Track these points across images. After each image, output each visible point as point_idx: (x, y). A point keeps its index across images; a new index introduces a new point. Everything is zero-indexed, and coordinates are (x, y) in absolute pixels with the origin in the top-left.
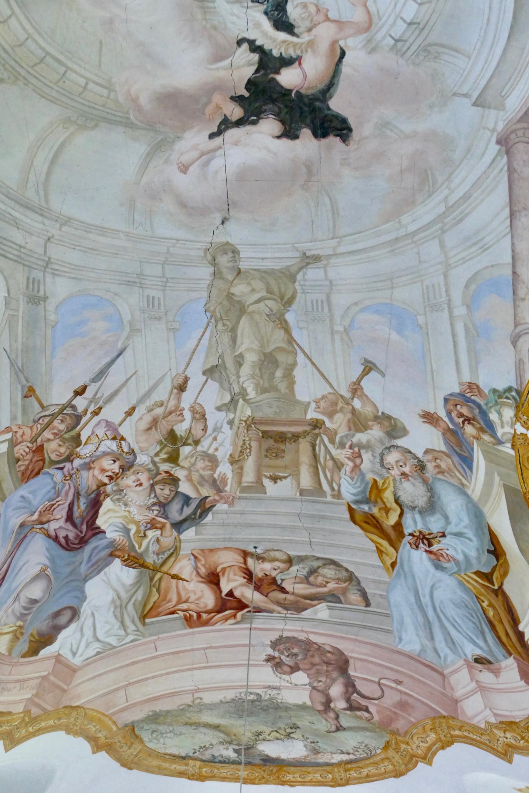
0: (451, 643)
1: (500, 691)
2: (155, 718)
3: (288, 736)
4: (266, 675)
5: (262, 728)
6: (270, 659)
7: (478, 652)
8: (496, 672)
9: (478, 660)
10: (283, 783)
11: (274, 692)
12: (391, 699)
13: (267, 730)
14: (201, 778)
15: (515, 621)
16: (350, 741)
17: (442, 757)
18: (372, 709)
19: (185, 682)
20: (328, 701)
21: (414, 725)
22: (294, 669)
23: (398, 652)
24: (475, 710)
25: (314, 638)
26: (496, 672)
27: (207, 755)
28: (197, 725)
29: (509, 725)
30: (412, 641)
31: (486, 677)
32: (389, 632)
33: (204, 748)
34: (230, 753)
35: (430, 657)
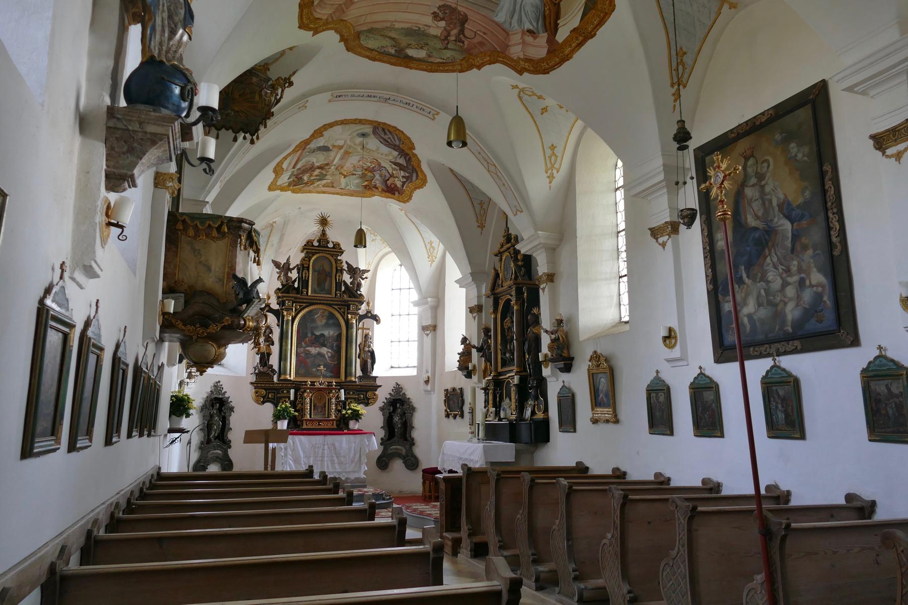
0: (520, 21)
1: (534, 46)
2: (371, 31)
3: (422, 48)
4: (429, 20)
5: (414, 43)
6: (434, 13)
7: (531, 28)
8: (535, 38)
9: (529, 31)
10: (407, 67)
11: (426, 28)
12: (477, 39)
13: (414, 43)
14: (374, 60)
15: (558, 16)
16: (448, 54)
17: (487, 68)
18: (466, 43)
19: (391, 17)
20: (449, 35)
21: (481, 52)
22: (442, 19)
23: (494, 22)
24: (516, 51)
25: (459, 8)
26: (535, 38)
27: (383, 50)
28: (386, 36)
29: (528, 60)
30: (501, 17)
31: (529, 39)
32: (494, 11)
33: (383, 47)
34: (393, 51)
35: (506, 26)
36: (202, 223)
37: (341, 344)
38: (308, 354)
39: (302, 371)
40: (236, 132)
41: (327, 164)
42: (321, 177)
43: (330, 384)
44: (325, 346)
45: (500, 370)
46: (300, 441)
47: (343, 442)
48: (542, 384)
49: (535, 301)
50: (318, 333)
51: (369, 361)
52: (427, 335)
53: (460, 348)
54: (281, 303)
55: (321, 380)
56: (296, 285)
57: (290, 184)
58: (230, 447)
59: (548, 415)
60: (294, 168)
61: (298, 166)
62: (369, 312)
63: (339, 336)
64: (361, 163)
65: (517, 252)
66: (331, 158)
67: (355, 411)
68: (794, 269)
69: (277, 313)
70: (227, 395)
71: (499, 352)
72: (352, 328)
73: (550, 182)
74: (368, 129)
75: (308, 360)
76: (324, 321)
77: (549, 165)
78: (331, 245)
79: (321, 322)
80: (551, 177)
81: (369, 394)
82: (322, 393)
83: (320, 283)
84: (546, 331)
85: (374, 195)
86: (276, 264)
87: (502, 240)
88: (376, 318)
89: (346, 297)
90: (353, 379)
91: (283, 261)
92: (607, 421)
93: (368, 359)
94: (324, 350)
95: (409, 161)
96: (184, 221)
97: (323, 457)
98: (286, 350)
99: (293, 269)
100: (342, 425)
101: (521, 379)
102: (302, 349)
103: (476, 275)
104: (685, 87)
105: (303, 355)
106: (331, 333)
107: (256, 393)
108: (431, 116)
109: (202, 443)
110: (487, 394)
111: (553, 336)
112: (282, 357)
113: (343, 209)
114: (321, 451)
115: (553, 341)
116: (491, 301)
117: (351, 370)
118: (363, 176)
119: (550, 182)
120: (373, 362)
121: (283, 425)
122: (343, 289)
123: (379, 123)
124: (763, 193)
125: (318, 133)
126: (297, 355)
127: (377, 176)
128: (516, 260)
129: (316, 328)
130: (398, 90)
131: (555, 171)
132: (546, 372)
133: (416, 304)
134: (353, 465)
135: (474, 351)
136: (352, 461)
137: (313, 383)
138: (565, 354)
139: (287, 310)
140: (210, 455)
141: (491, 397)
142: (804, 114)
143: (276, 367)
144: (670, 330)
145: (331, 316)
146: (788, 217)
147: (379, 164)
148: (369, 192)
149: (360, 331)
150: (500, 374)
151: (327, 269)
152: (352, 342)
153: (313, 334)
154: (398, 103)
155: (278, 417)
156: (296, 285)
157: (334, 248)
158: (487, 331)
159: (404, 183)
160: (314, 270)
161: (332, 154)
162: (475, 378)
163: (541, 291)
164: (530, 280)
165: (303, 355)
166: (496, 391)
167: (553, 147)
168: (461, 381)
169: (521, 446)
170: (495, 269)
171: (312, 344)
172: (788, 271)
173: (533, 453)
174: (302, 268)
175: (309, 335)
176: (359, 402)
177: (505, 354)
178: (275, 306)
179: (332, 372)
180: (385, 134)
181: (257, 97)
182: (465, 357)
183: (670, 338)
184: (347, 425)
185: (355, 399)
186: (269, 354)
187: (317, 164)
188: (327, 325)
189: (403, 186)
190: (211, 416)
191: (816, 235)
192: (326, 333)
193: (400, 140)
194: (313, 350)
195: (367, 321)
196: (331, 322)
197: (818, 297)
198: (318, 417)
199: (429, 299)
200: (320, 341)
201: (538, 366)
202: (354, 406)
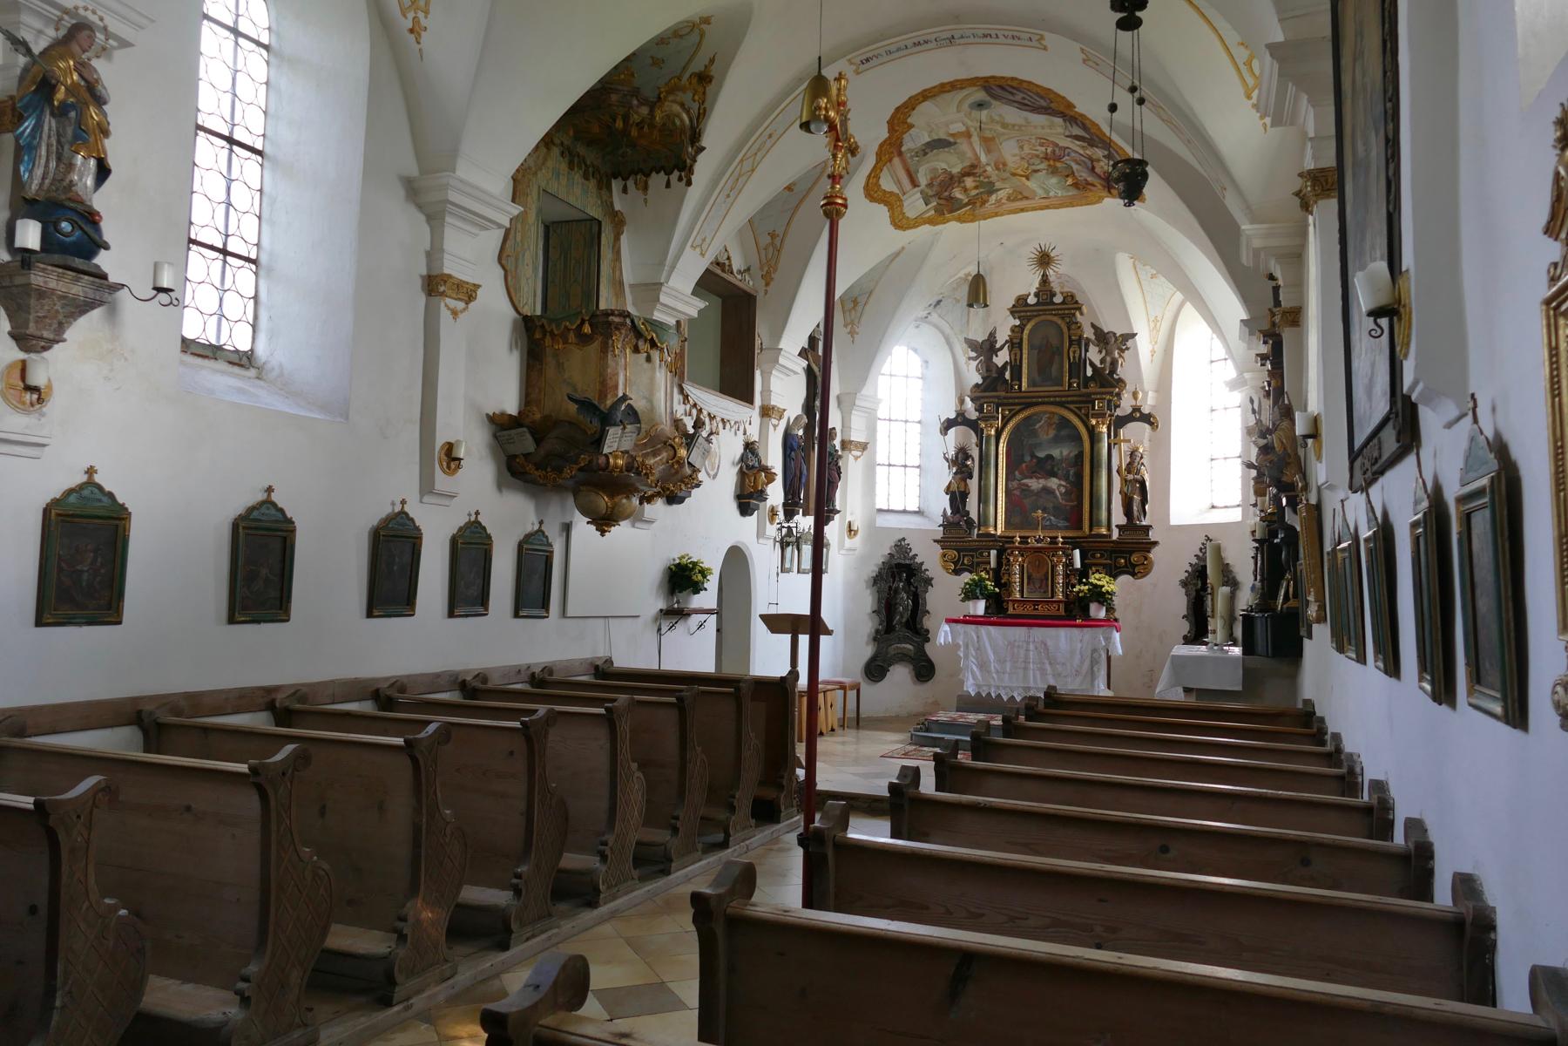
36: (558, 326)
37: (1081, 472)
38: (1026, 490)
39: (1016, 520)
40: (668, 173)
41: (973, 166)
42: (991, 190)
43: (1054, 539)
44: (1055, 475)
46: (989, 634)
47: (1064, 640)
50: (1041, 454)
51: (1137, 498)
54: (980, 409)
55: (1040, 534)
56: (1007, 375)
57: (939, 211)
58: (928, 640)
60: (915, 184)
61: (923, 181)
62: (1136, 409)
63: (1080, 455)
64: (1027, 150)
66: (970, 154)
67: (1096, 586)
69: (973, 425)
70: (918, 560)
72: (1100, 440)
74: (981, 95)
75: (1027, 502)
76: (1052, 433)
77: (1250, 81)
78: (1058, 299)
79: (1046, 433)
81: (1134, 558)
82: (1039, 556)
83: (1043, 369)
85: (1100, 200)
86: (972, 344)
89: (1093, 387)
90: (1104, 531)
91: (981, 337)
93: (1137, 493)
94: (1053, 483)
95: (1084, 128)
96: (543, 326)
97: (1026, 662)
98: (987, 486)
99: (1001, 348)
100: (1075, 612)
102: (1015, 484)
105: (1017, 492)
106: (1065, 453)
107: (944, 555)
108: (1034, 43)
109: (877, 631)
112: (983, 498)
113: (1080, 231)
114: (1022, 652)
117: (1099, 515)
118: (1054, 171)
120: (1144, 501)
121: (980, 607)
122: (1089, 372)
123: (986, 79)
125: (899, 121)
126: (1008, 492)
127: (1075, 167)
129: (1038, 445)
130: (957, 18)
133: (1234, 385)
134: (1079, 679)
136: (1078, 673)
137: (1024, 539)
139: (985, 419)
140: (892, 650)
143: (974, 515)
145: (1065, 423)
151: (1054, 342)
152: (1099, 466)
153: (1033, 456)
154: (972, 40)
155: (970, 594)
156: (1007, 375)
157: (1063, 303)
160: (1031, 347)
161: (963, 146)
165: (1017, 492)
171: (1032, 474)
174: (1014, 344)
175: (1028, 458)
176: (1114, 573)
178: (973, 415)
179: (1066, 519)
181: (619, 124)
184: (1086, 610)
185: (1104, 566)
186: (964, 495)
187: (956, 170)
188: (1057, 440)
190: (896, 591)
192: (1056, 453)
194: (1035, 484)
196: (1063, 433)
198: (1036, 597)
199: (1247, 376)
200: (1046, 467)
202: (1099, 579)
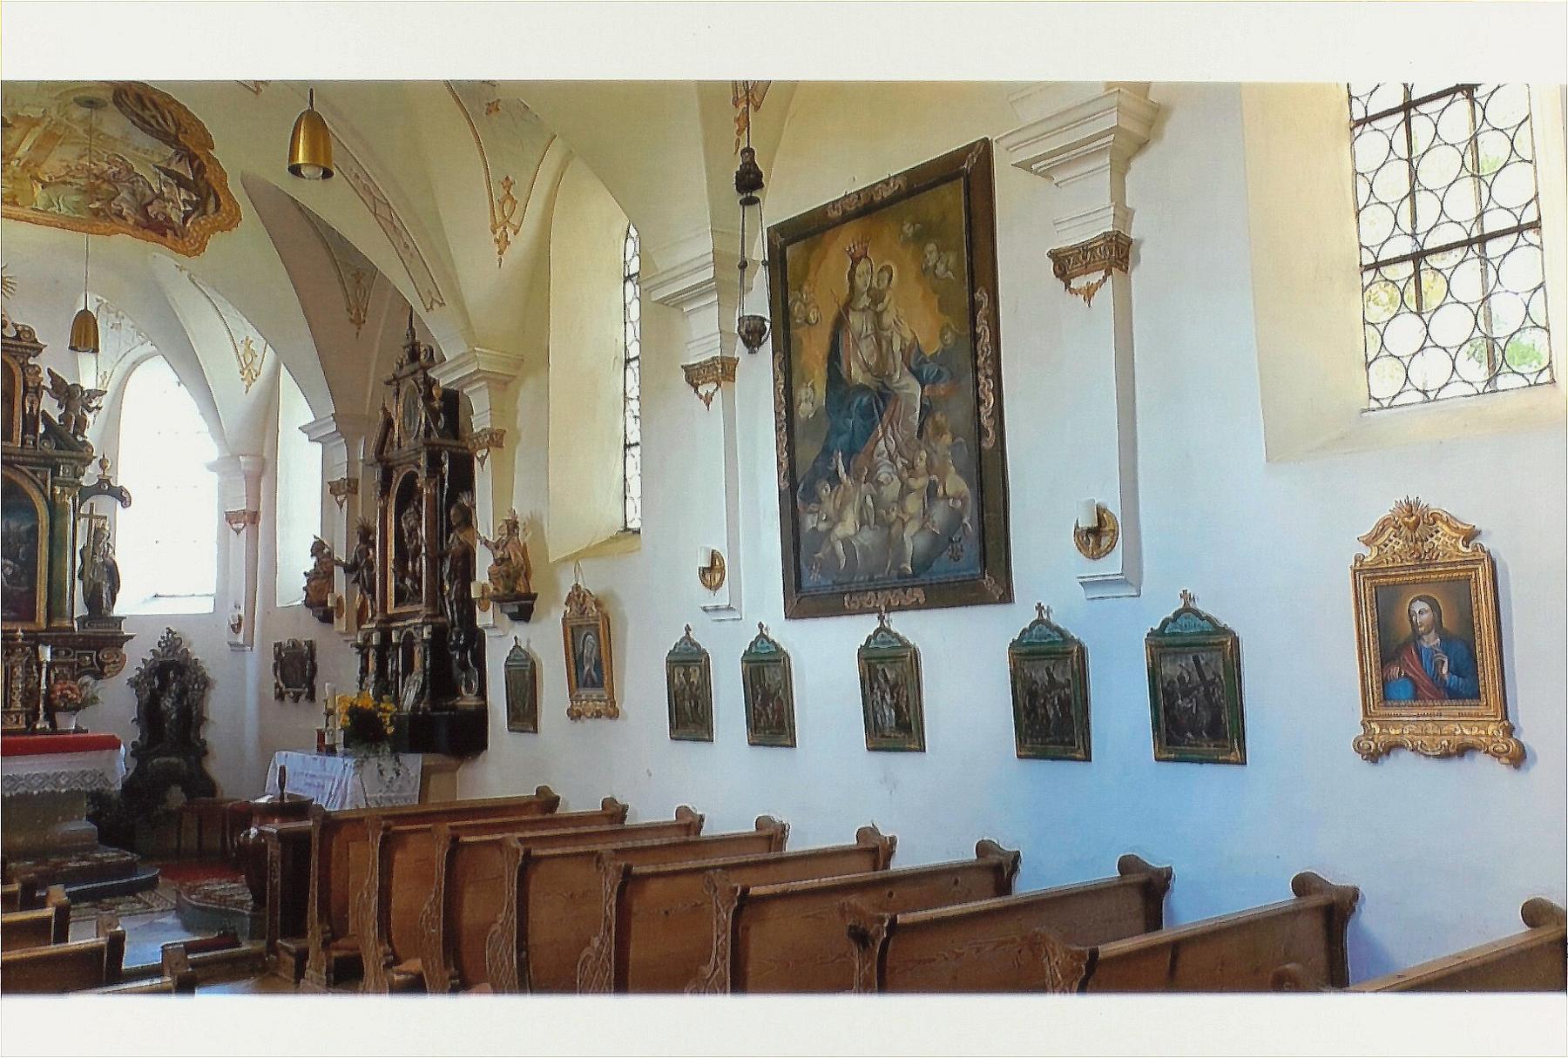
45: (391, 609)
48: (475, 641)
49: (463, 480)
52: (238, 531)
53: (309, 564)
59: (484, 698)
62: (103, 481)
63: (33, 532)
65: (430, 383)
68: (921, 465)
71: (390, 574)
73: (501, 253)
77: (499, 218)
80: (503, 243)
81: (104, 655)
84: (486, 543)
87: (404, 355)
88: (121, 496)
89: (48, 447)
90: (67, 623)
92: (598, 715)
101: (434, 633)
103: (343, 423)
104: (757, 108)
110: (365, 658)
111: (499, 554)
115: (499, 562)
116: (377, 474)
119: (501, 253)
120: (115, 585)
124: (878, 326)
127: (124, 194)
128: (428, 398)
131: (510, 232)
132: (483, 619)
135: (339, 572)
138: (520, 588)
141: (372, 665)
142: (952, 197)
144: (714, 556)
146: (917, 374)
147: (130, 170)
148: (103, 225)
149: (82, 523)
150: (393, 618)
157: (18, 338)
158: (365, 534)
159: (187, 216)
162: (340, 624)
163: (477, 464)
164: (457, 437)
166: (382, 658)
167: (508, 184)
168: (308, 629)
169: (433, 759)
170: (385, 410)
172: (911, 467)
173: (454, 770)
177: (403, 581)
180: (144, 107)
182: (319, 579)
183: (712, 572)
189: (185, 220)
191: (955, 413)
193: (178, 125)
195: (102, 504)
197: (956, 516)
201: (467, 607)
